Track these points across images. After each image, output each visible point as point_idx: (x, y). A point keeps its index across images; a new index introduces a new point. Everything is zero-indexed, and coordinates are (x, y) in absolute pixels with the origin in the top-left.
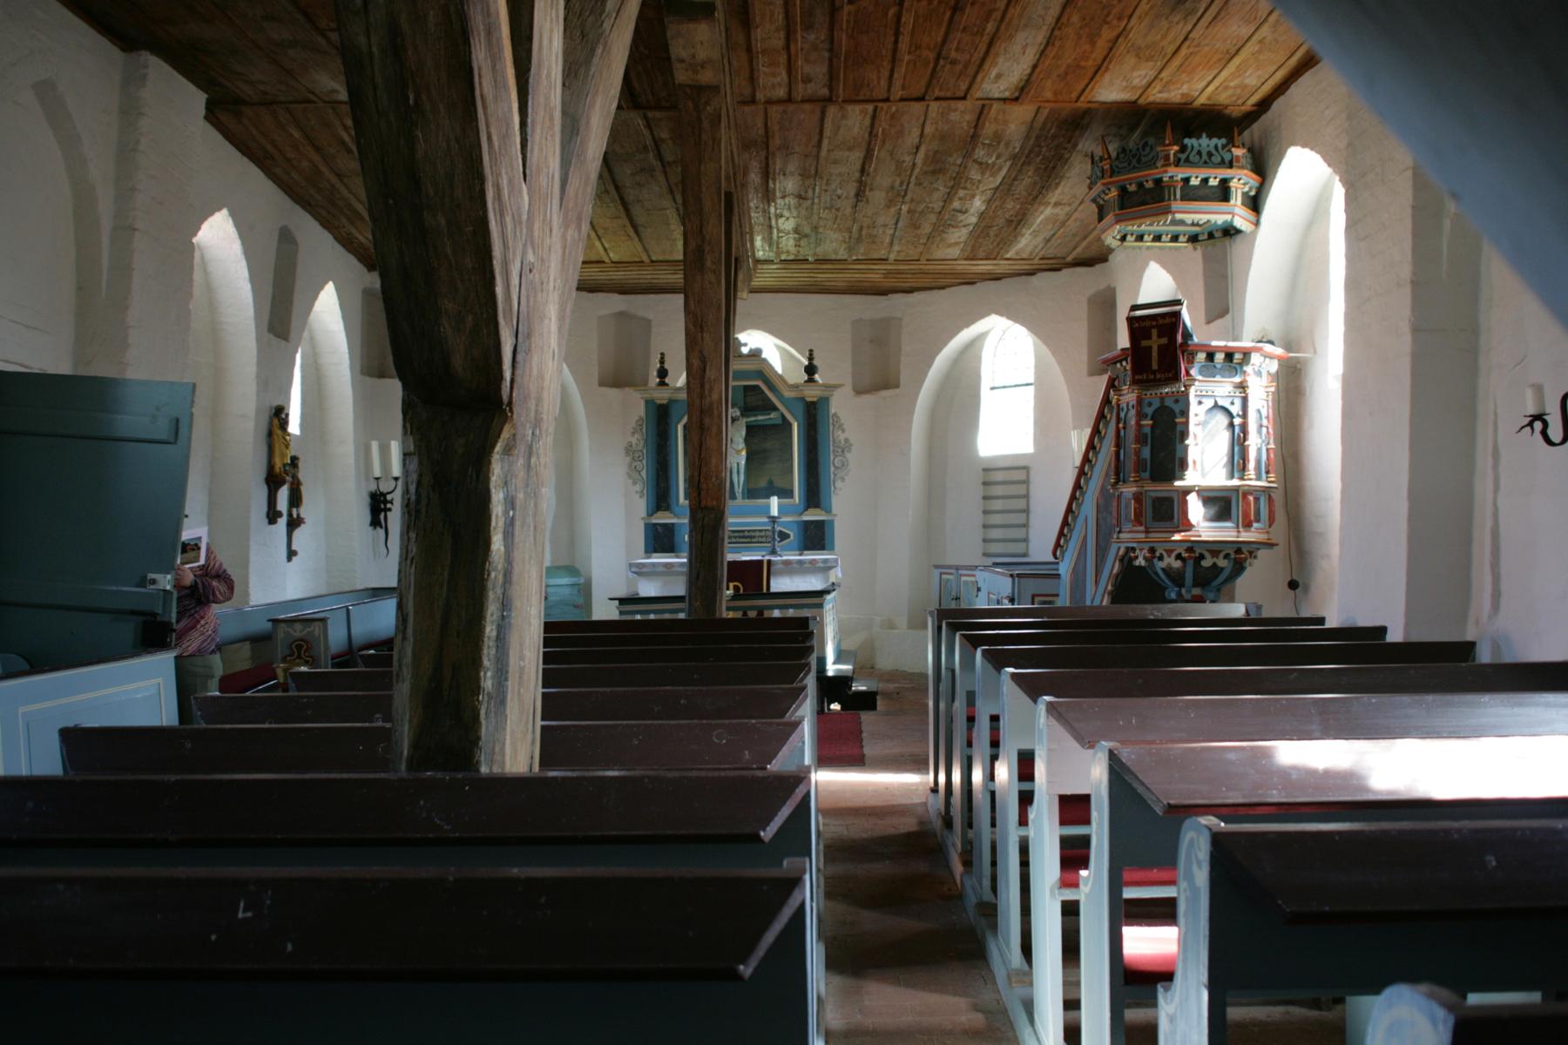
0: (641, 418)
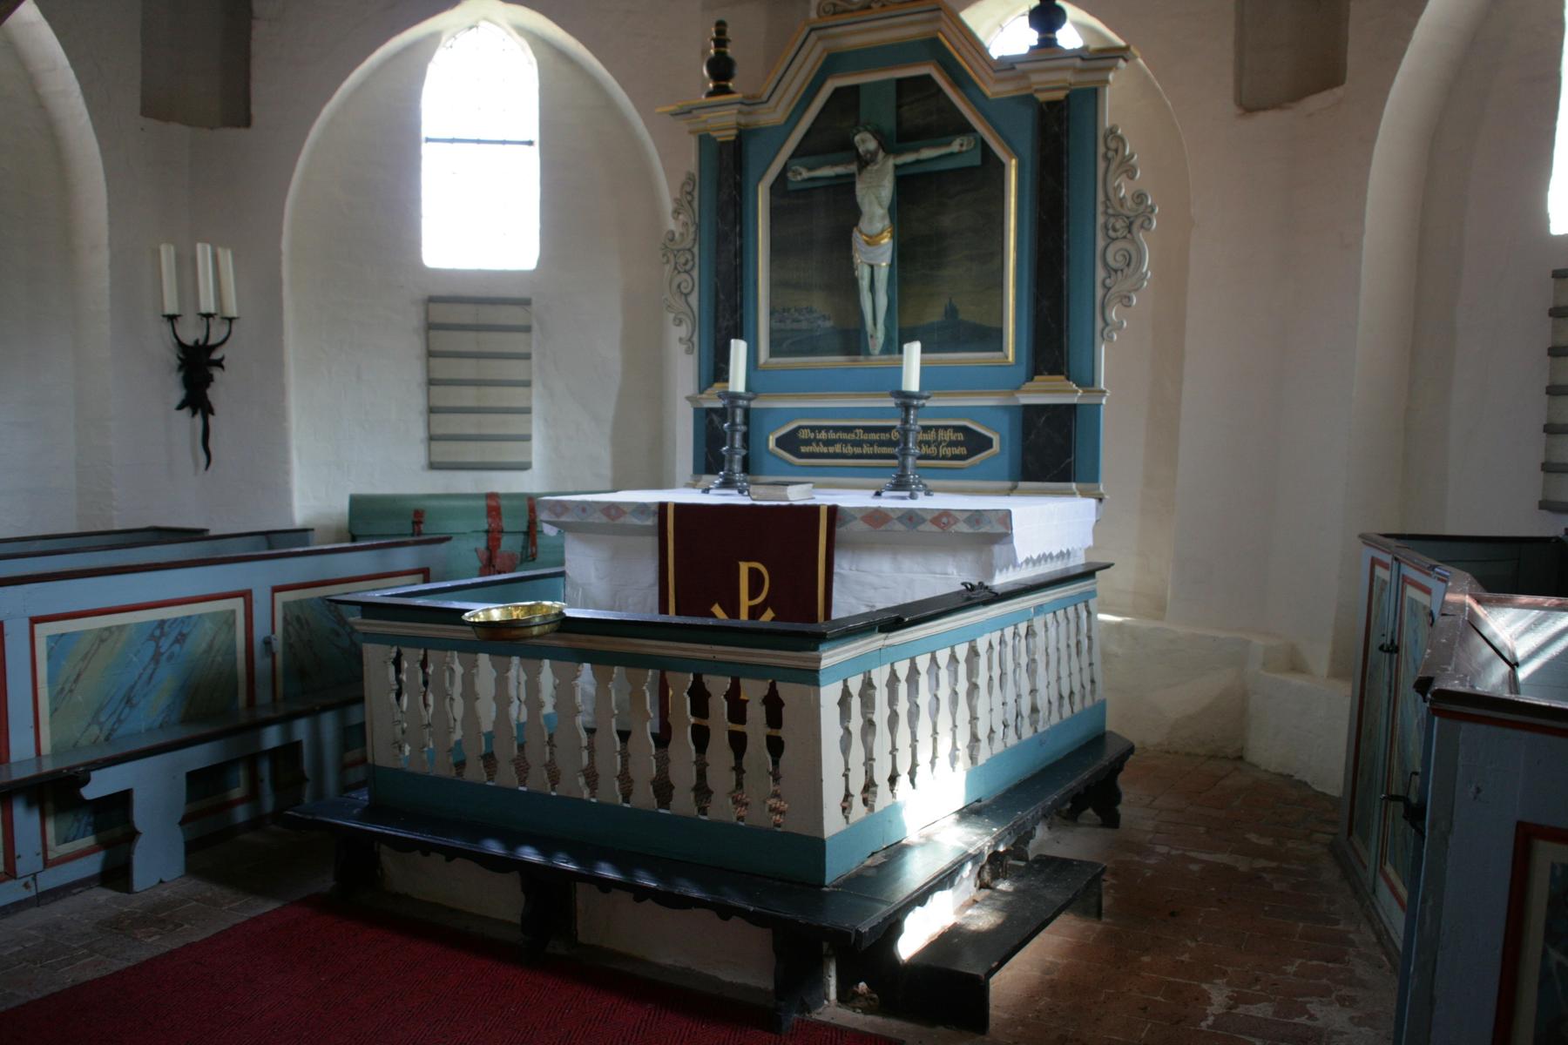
0: (690, 177)
